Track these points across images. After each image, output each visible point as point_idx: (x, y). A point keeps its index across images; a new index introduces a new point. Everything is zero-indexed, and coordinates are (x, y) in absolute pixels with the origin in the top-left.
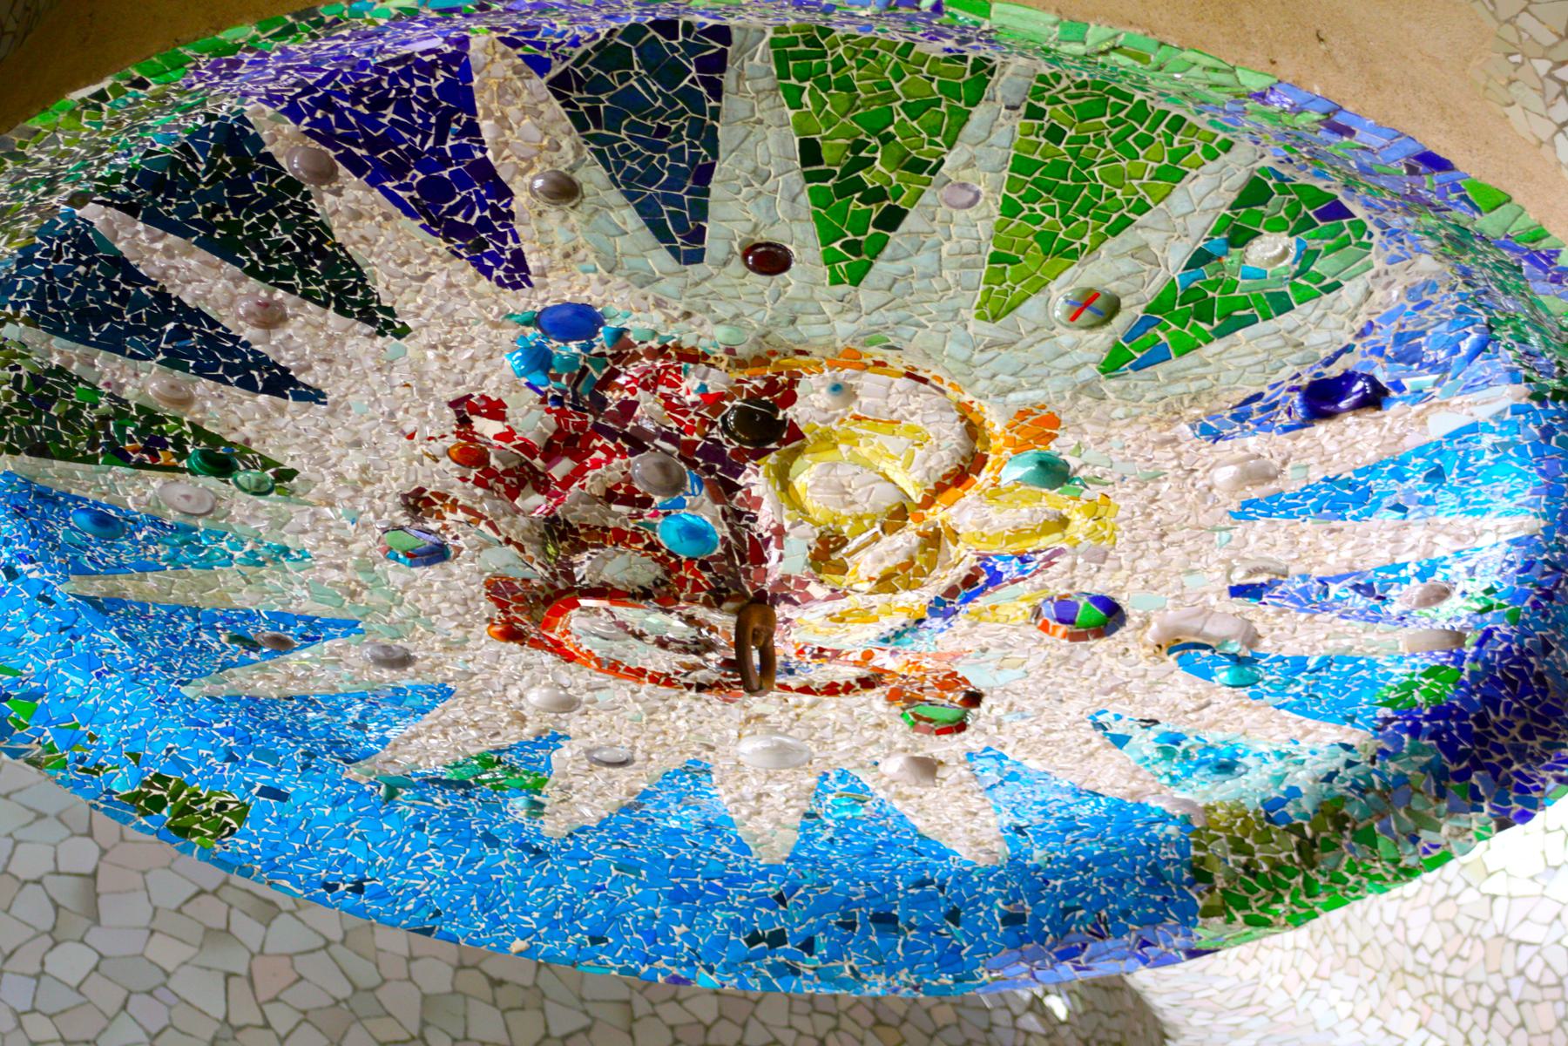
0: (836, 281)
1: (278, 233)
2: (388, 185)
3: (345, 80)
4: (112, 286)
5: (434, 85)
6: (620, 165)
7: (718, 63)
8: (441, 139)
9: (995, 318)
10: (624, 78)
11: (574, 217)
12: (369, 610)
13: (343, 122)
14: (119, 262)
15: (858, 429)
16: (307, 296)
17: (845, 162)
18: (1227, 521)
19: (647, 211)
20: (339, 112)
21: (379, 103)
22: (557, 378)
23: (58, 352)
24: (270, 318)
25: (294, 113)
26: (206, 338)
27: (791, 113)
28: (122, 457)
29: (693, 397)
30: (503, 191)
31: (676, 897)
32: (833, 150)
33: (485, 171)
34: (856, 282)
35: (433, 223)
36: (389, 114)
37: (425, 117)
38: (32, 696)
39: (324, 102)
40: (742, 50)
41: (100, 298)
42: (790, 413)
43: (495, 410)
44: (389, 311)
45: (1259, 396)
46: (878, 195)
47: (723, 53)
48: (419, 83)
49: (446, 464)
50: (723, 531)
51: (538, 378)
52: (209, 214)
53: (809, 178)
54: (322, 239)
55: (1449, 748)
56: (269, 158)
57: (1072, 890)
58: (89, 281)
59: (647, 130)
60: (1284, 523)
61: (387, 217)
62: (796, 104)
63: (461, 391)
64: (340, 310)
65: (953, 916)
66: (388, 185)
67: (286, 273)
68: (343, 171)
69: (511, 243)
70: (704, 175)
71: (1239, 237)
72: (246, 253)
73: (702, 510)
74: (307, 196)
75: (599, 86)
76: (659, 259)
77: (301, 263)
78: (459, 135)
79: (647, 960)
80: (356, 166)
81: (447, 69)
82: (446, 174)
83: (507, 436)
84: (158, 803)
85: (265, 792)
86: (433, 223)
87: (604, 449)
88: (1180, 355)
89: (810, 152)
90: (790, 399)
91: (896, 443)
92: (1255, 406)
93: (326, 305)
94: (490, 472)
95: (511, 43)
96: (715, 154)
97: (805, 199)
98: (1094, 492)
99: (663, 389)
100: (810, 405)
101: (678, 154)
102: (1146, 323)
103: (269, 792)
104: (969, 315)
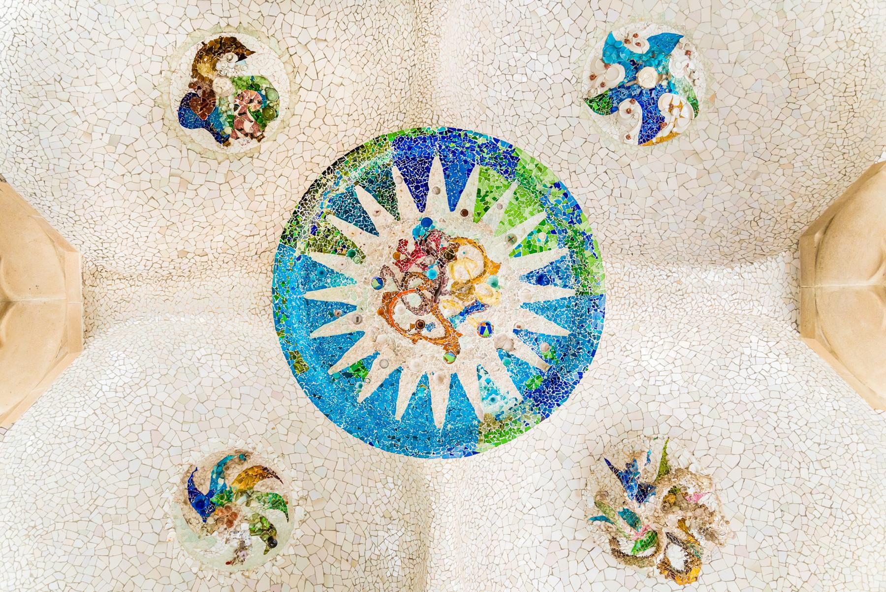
1: (387, 194)
14: (356, 199)
23: (334, 221)
25: (400, 169)
30: (428, 189)
31: (377, 424)
32: (482, 194)
33: (426, 185)
38: (287, 317)
39: (406, 167)
46: (487, 203)
55: (536, 400)
57: (453, 436)
65: (429, 439)
71: (539, 231)
79: (367, 436)
80: (406, 180)
84: (295, 357)
85: (313, 368)
89: (479, 191)
90: (457, 251)
91: (472, 266)
94: (399, 261)
95: (441, 160)
102: (519, 246)
103: (313, 368)
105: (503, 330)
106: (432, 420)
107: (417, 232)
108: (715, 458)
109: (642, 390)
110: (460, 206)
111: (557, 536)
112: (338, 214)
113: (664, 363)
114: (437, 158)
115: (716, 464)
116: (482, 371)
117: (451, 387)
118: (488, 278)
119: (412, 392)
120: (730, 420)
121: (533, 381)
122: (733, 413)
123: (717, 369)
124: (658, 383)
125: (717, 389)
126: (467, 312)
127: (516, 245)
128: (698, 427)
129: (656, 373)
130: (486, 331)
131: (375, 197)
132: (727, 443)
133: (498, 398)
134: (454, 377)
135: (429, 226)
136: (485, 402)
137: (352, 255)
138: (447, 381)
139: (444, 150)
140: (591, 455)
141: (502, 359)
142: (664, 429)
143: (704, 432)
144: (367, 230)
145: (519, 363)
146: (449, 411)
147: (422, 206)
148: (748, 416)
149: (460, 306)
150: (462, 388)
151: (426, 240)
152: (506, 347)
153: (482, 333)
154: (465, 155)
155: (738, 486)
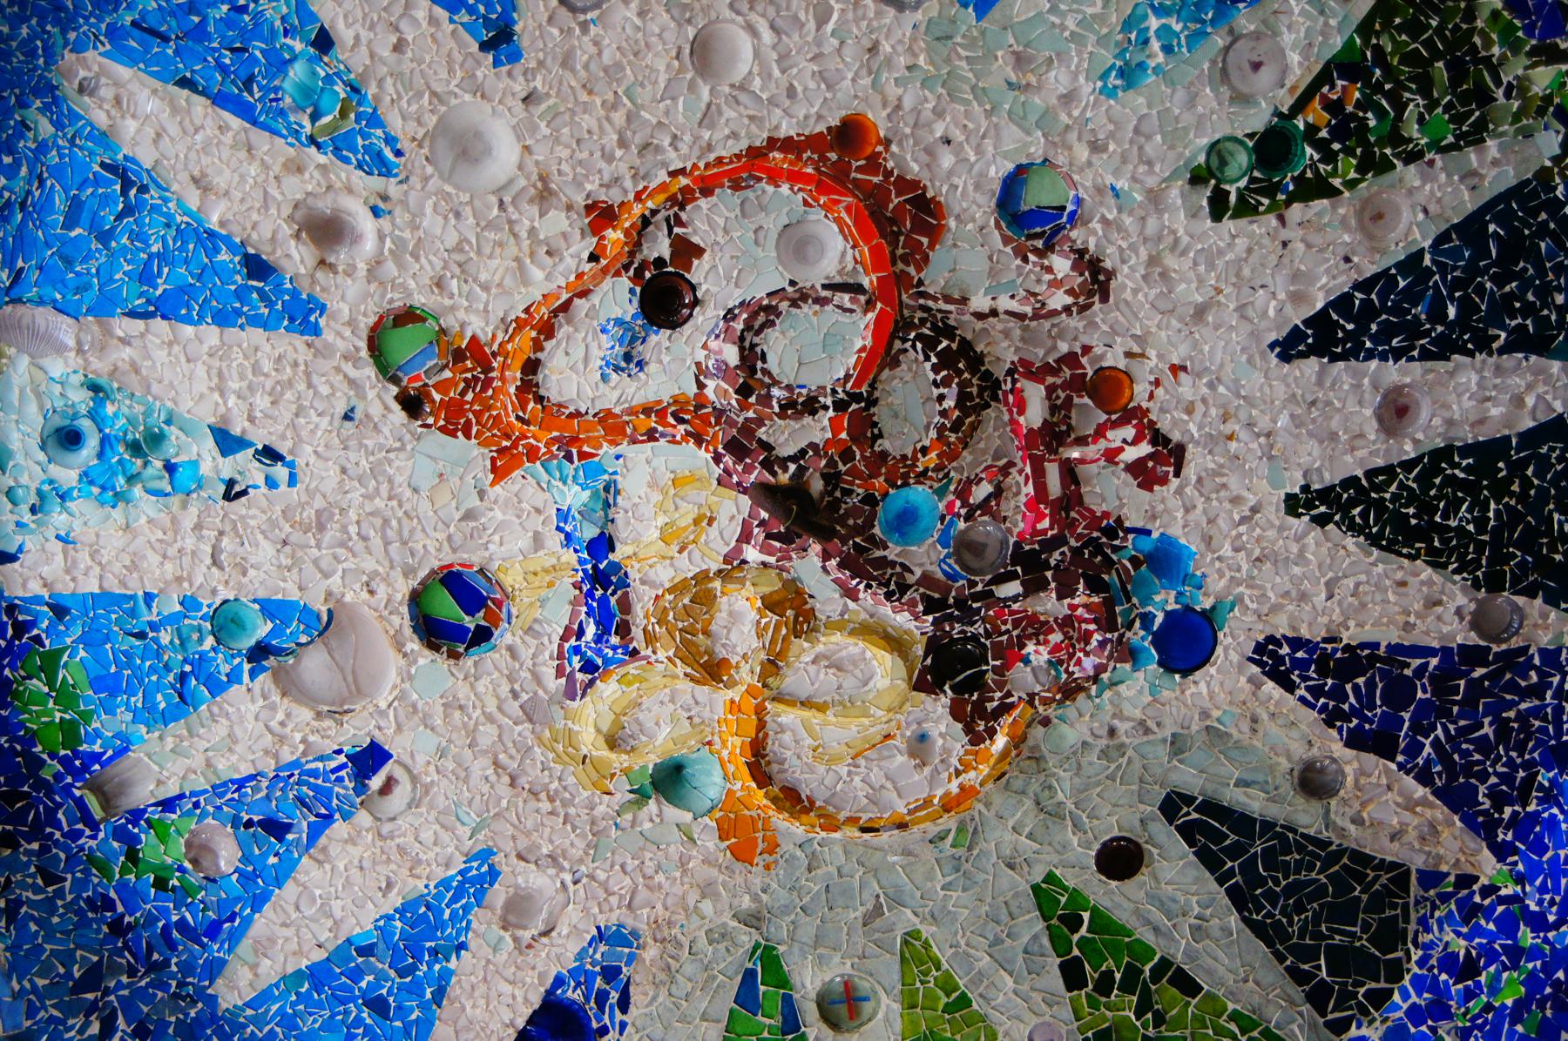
0: (1050, 878)
2: (1434, 662)
3: (1544, 730)
4: (1528, 310)
5: (1482, 789)
6: (1301, 849)
7: (1318, 998)
8: (1436, 744)
9: (905, 942)
10: (1365, 929)
11: (1285, 764)
12: (991, 56)
13: (1512, 687)
15: (882, 729)
16: (1389, 471)
17: (1155, 997)
18: (482, 841)
19: (1242, 822)
20: (1525, 693)
21: (1502, 727)
22: (1133, 560)
23: (1497, 165)
24: (1395, 411)
26: (1413, 331)
27: (1231, 1006)
28: (1344, 66)
29: (1030, 648)
30: (1355, 741)
34: (1036, 889)
35: (1373, 658)
36: (1487, 730)
37: (1465, 754)
39: (1537, 691)
40: (1313, 1026)
41: (1523, 288)
42: (945, 700)
43: (1145, 476)
44: (1321, 521)
45: (624, 1004)
46: (1104, 985)
47: (1323, 1014)
48: (1493, 780)
49: (1114, 359)
50: (892, 552)
51: (1146, 544)
52: (1526, 484)
53: (1165, 964)
54: (1431, 551)
56: (1531, 593)
58: (1545, 292)
59: (1312, 898)
60: (441, 873)
61: (1408, 627)
62: (1235, 1017)
63: (1190, 471)
64: (1351, 482)
66: (1434, 662)
67: (1424, 480)
68: (1473, 639)
69: (1302, 692)
70: (1238, 898)
72: (1466, 470)
73: (925, 556)
74: (1476, 585)
75: (1377, 903)
76: (1189, 779)
77: (1426, 508)
78: (1428, 761)
80: (1473, 655)
81: (1485, 813)
82: (1406, 716)
83: (1111, 456)
86: (1373, 658)
87: (1045, 531)
88: (731, 1011)
89: (1187, 985)
90: (956, 712)
92: (614, 996)
93: (1371, 474)
94: (1078, 384)
95: (1466, 880)
96: (1247, 921)
97: (1149, 938)
98: (622, 795)
99: (1056, 637)
100: (936, 713)
101: (1272, 897)
104: (927, 931)
105: (407, 694)
106: (131, 59)
107: (1164, 561)
110: (1174, 867)
112: (1529, 195)
114: (1488, 867)
116: (252, 471)
117: (257, 267)
118: (715, 780)
119: (343, 33)
121: (65, 697)
126: (602, 577)
127: (809, 1012)
130: (446, 607)
131: (1488, 452)
133: (68, 476)
134: (303, 315)
135: (1159, 640)
136: (80, 398)
137: (1273, 147)
138: (295, 258)
139: (1508, 926)
141: (269, 608)
144: (1342, 303)
145: (191, 686)
146: (122, 172)
147: (1276, 660)
149: (652, 567)
150: (223, 319)
151: (1095, 585)
152: (315, 665)
153: (458, 583)
154: (1415, 1014)
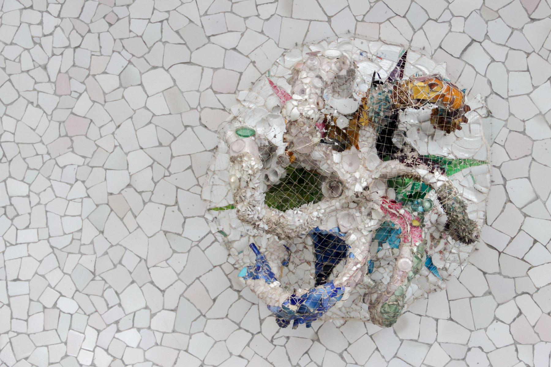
108: (200, 108)
109: (142, 319)
111: (500, 335)
113: (65, 319)
115: (210, 99)
120: (111, 127)
122: (93, 132)
123: (20, 222)
124: (113, 300)
125: (61, 189)
128: (159, 171)
129: (95, 320)
132: (158, 105)
140: (316, 339)
142: (196, 229)
143: (162, 155)
148: (82, 106)
155: (230, 40)
